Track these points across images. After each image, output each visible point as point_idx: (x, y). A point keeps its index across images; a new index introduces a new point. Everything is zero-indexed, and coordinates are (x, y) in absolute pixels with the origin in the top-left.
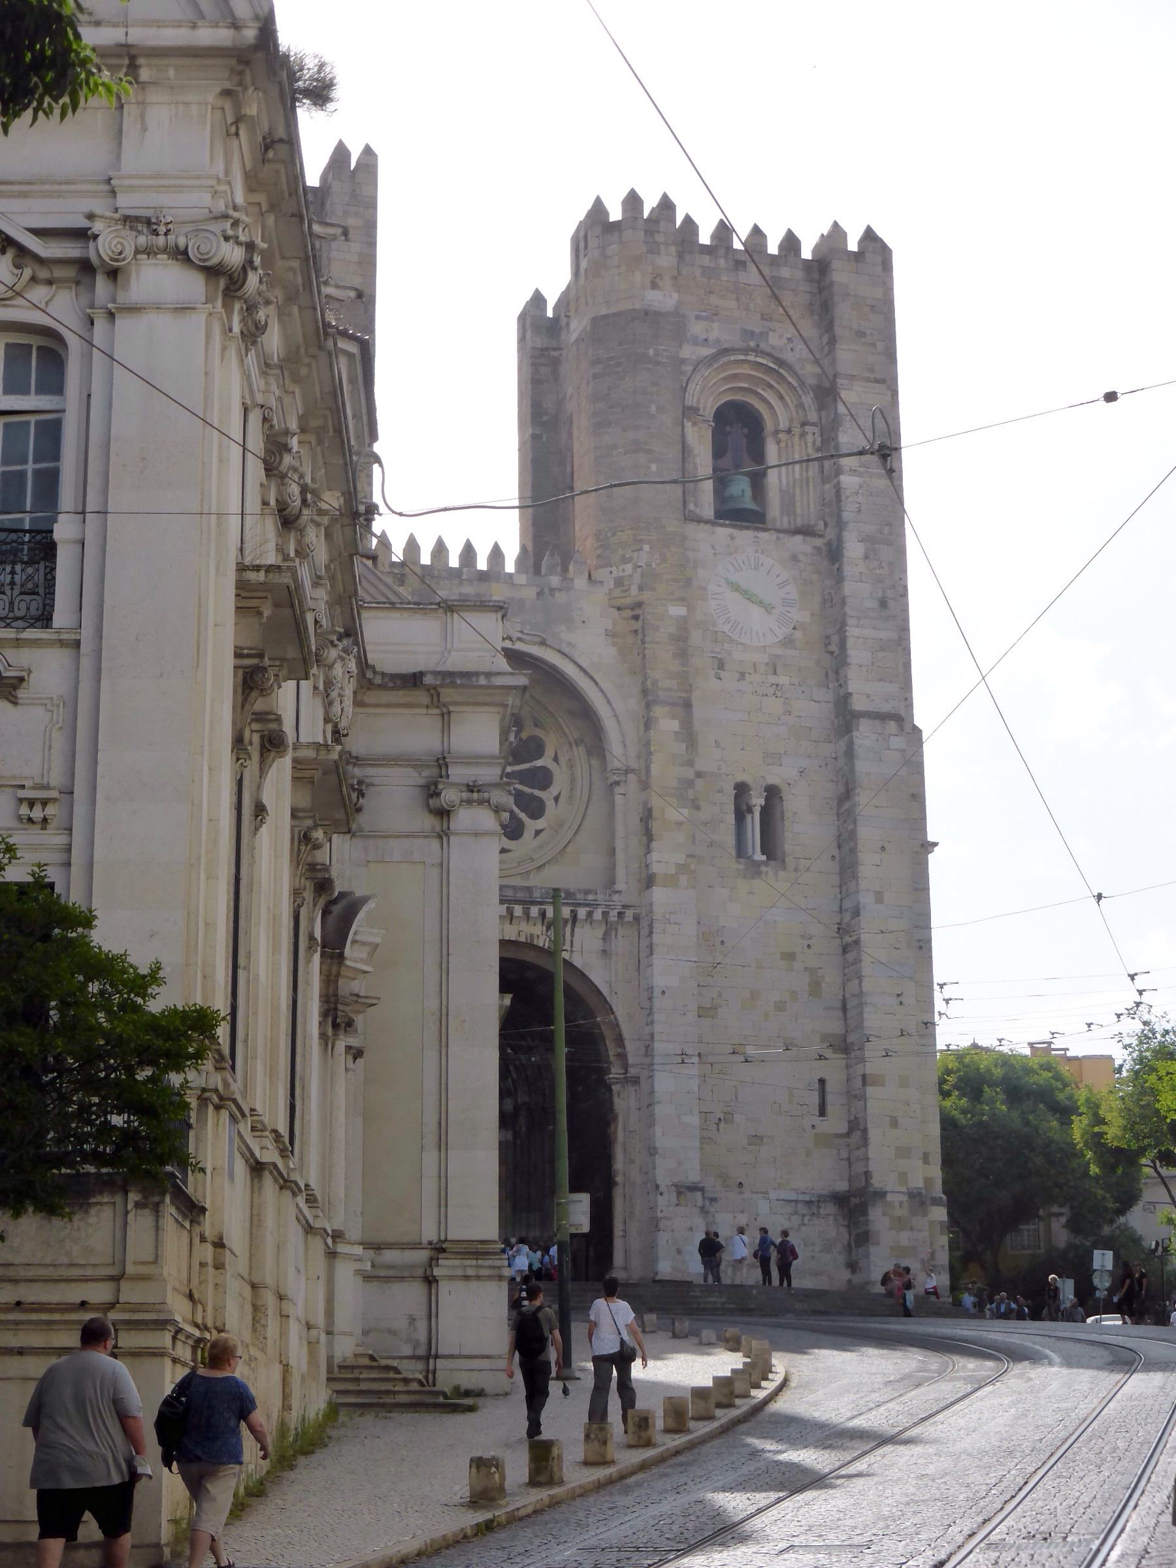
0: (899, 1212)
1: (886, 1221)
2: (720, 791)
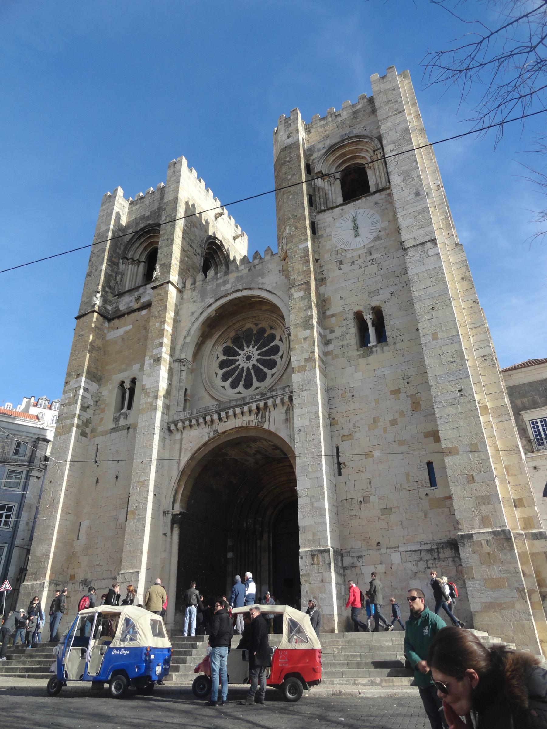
0: (487, 549)
1: (476, 556)
2: (346, 319)
